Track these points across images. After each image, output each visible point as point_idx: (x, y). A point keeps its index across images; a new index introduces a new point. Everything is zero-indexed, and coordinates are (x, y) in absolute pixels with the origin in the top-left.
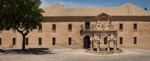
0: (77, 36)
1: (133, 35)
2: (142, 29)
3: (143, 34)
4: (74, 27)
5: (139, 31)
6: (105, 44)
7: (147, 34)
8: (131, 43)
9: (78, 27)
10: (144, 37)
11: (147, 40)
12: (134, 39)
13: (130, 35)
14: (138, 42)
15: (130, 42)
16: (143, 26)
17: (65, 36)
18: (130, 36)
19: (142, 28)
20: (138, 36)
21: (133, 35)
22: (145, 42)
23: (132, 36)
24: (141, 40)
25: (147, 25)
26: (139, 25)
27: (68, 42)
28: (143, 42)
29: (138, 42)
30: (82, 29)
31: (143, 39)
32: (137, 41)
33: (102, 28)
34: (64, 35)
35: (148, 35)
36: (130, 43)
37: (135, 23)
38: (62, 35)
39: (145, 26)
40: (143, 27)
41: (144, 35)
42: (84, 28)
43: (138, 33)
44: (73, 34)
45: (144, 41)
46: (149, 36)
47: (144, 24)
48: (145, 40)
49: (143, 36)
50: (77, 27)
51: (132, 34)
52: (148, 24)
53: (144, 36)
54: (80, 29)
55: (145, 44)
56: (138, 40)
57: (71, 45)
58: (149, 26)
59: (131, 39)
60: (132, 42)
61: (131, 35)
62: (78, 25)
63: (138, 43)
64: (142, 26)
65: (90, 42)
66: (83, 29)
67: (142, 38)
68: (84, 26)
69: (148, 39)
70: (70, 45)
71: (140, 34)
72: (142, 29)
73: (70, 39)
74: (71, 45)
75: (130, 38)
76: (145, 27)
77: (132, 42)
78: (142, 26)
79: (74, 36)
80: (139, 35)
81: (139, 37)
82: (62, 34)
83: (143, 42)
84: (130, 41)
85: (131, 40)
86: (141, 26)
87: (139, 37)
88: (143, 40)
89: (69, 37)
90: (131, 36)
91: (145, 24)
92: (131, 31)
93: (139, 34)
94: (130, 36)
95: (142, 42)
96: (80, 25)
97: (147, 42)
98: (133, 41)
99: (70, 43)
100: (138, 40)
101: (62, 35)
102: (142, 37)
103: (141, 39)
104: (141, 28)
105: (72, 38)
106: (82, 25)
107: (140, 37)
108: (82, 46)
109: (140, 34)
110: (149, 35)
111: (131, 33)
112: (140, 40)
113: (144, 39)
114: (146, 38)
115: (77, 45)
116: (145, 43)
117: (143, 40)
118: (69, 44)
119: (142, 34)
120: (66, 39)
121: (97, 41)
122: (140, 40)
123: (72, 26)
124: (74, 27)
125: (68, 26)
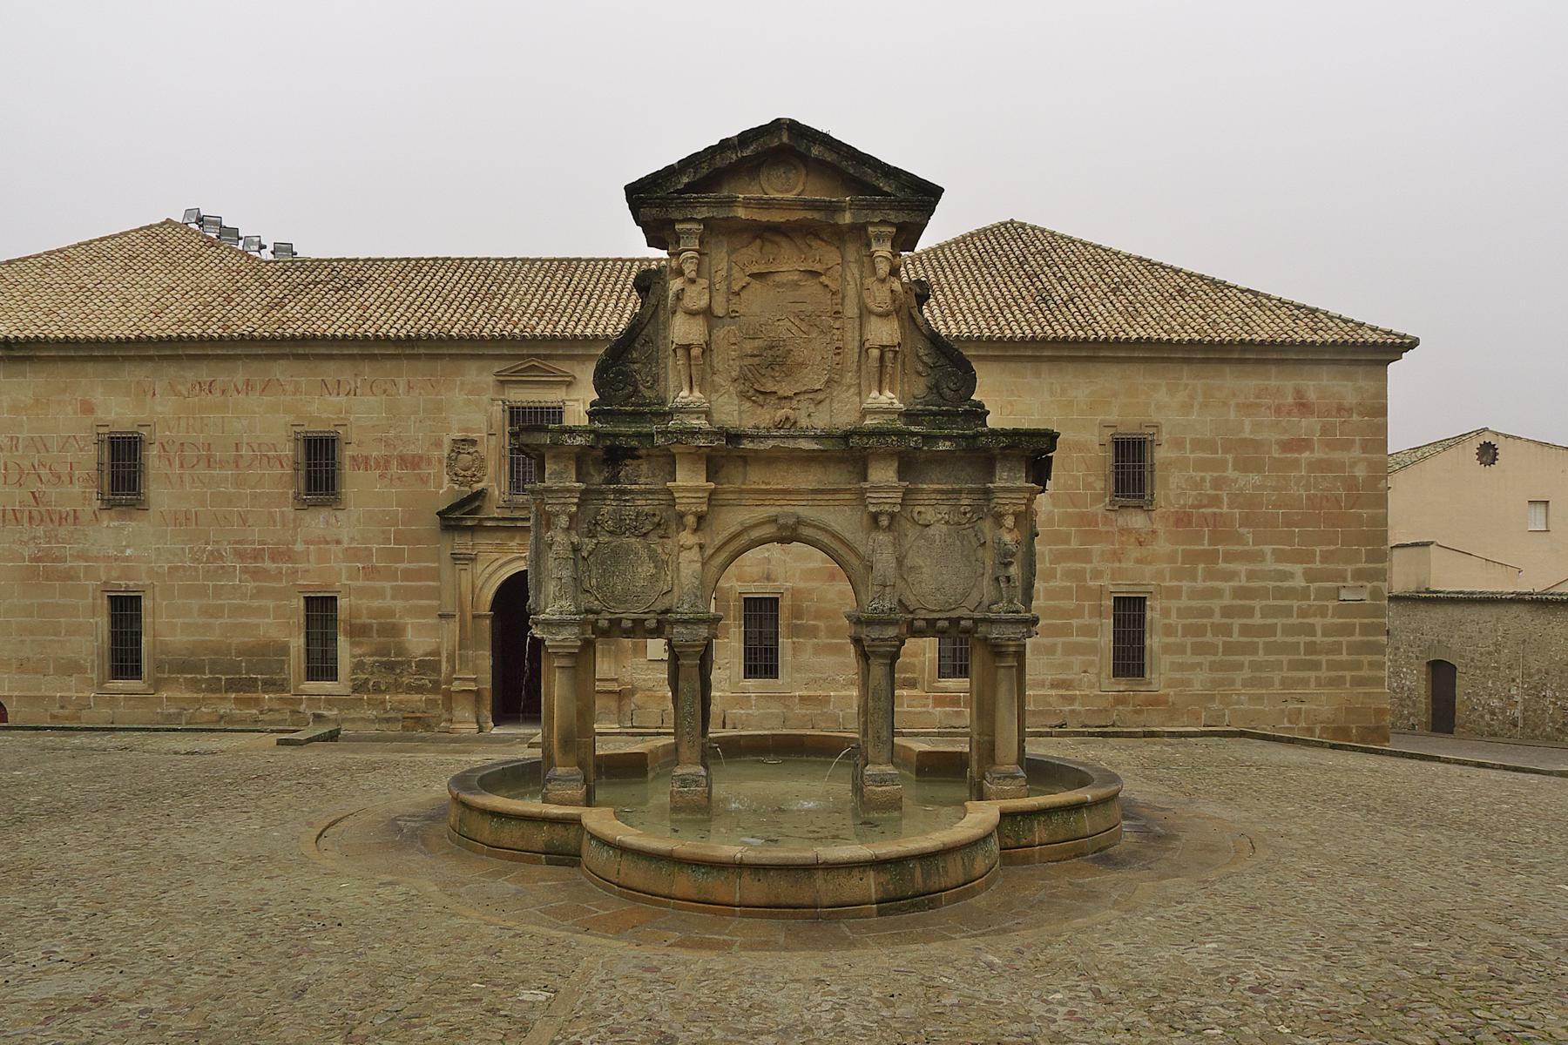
0: (407, 574)
1: (1096, 563)
2: (1215, 501)
3: (1230, 557)
4: (364, 462)
5: (1182, 519)
6: (750, 672)
7: (1280, 556)
8: (1077, 660)
9: (425, 471)
10: (1239, 593)
11: (1270, 631)
12: (1117, 621)
13: (1060, 568)
14: (1167, 649)
15: (1071, 649)
16: (1230, 457)
17: (256, 574)
18: (1068, 574)
19: (1217, 484)
20: (1159, 575)
21: (1096, 563)
22: (1251, 649)
23: (1097, 574)
24: (1199, 631)
25: (1276, 453)
26: (1173, 455)
27: (297, 643)
28: (1229, 649)
29: (1167, 649)
30: (467, 491)
31: (1227, 612)
32: (1153, 642)
33: (757, 395)
34: (241, 555)
35: (1289, 575)
36: (1067, 666)
37: (1121, 430)
38: (217, 555)
39: (1244, 466)
40: (1230, 473)
41: (1242, 568)
42: (495, 482)
43: (1168, 547)
44: (351, 554)
45: (1236, 638)
46: (1299, 582)
47: (1245, 443)
48: (1245, 630)
49: (1231, 576)
50: (403, 461)
51: (1085, 556)
52: (1286, 446)
53: (1243, 582)
54: (445, 490)
55: (1247, 673)
56: (1169, 630)
57: (330, 673)
58: (1295, 464)
59: (1077, 612)
60: (1092, 649)
61: (1078, 566)
62: (411, 450)
63: (1167, 659)
64: (1220, 465)
65: (538, 643)
66: (480, 495)
67: (1216, 604)
68: (493, 451)
69: (1287, 612)
70: (327, 686)
71: (1192, 557)
72: (1215, 501)
73: (320, 610)
74: (330, 673)
75: (1071, 604)
76: (1255, 478)
77: (1092, 649)
78: (1220, 465)
79: (370, 573)
80: (1178, 574)
81: (1175, 593)
82: (226, 548)
83: (1229, 649)
84: (1060, 640)
85: (1075, 622)
86: (1201, 465)
87: (1175, 593)
88: (1225, 630)
89: (314, 582)
90: (1077, 575)
91: (1256, 444)
92: (1084, 520)
93: (1171, 558)
94: (1068, 574)
95: (1208, 649)
96: (438, 444)
97: (1269, 649)
98: (1106, 639)
99: (321, 666)
100: (1169, 630)
101: (217, 555)
102: (1216, 593)
103: (1209, 613)
104: (1197, 485)
105: (342, 603)
106: (473, 442)
107: (1194, 594)
108: (478, 693)
109: (1192, 557)
110: (1298, 569)
111: (1074, 545)
112: (1188, 630)
113: (1237, 623)
114: (1257, 604)
115: (406, 680)
116: (1246, 659)
117: (1225, 630)
118: (313, 674)
119: (1210, 557)
120: (270, 603)
121: (657, 632)
122: (1188, 630)
123: (349, 452)
124: (364, 462)
125: (287, 450)
